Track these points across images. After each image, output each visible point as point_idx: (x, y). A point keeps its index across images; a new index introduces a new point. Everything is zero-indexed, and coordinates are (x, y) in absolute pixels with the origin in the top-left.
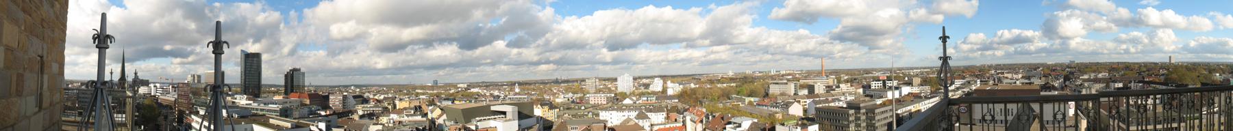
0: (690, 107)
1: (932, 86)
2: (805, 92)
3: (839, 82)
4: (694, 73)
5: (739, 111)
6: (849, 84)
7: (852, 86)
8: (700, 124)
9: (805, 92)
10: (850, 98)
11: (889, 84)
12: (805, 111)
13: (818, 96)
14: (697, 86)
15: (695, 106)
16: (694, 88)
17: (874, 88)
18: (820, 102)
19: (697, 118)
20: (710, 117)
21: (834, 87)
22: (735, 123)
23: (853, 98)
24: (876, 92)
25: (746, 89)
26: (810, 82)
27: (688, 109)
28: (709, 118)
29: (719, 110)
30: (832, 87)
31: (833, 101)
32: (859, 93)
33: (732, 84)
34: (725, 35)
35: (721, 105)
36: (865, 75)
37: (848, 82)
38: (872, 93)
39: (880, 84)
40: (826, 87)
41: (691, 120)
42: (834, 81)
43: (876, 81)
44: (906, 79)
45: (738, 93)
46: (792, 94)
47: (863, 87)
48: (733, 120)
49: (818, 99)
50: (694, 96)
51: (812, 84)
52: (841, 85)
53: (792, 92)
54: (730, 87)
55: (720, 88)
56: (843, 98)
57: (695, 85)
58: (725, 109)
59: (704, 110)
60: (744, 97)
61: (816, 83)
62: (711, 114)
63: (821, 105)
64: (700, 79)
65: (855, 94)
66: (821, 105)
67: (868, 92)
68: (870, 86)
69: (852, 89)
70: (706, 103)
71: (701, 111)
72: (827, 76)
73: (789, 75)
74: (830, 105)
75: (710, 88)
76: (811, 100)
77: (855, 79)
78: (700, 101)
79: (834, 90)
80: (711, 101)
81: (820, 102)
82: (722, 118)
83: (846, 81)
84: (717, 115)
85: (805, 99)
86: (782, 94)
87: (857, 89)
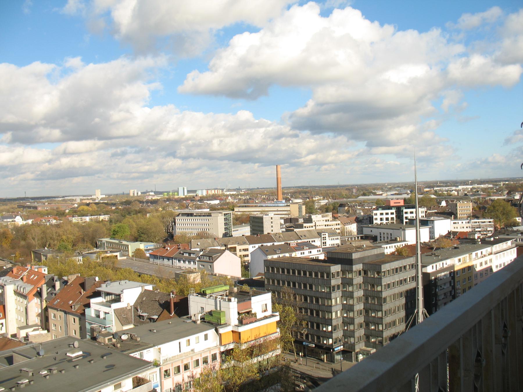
0: (14, 265)
1: (497, 218)
2: (246, 230)
3: (311, 210)
4: (23, 196)
5: (116, 269)
6: (330, 215)
7: (335, 218)
8: (36, 300)
9: (246, 230)
10: (331, 242)
11: (408, 214)
12: (246, 267)
13: (269, 238)
14: (30, 222)
15: (24, 264)
16: (23, 226)
17: (379, 222)
18: (274, 250)
19: (28, 288)
20: (58, 285)
21: (301, 221)
22: (108, 294)
23: (338, 242)
24: (382, 231)
25: (131, 227)
26: (254, 211)
27: (11, 269)
28: (54, 287)
29: (74, 268)
30: (296, 220)
31: (300, 247)
32: (350, 233)
33: (102, 217)
34: (97, 120)
35: (79, 260)
36: (361, 198)
37: (327, 211)
38: (375, 232)
39: (391, 214)
40: (286, 221)
41: (17, 293)
42: (300, 209)
43: (384, 208)
44: (444, 204)
45: (114, 234)
46: (221, 236)
47: (358, 221)
48: (103, 288)
49: (269, 244)
50: (23, 243)
51: (259, 215)
52: (313, 217)
53: (221, 231)
54: (98, 222)
55: (77, 225)
56: (318, 242)
57: (25, 218)
58: (88, 265)
59: (45, 271)
60: (124, 243)
61: (266, 213)
62: (60, 279)
63: (275, 256)
64: (36, 208)
65: (342, 234)
66: (275, 256)
67: (367, 231)
68: (370, 220)
69: (336, 225)
70: (49, 255)
71: (39, 274)
72: (287, 200)
73: (214, 197)
74: (294, 255)
75: (58, 226)
76: (257, 246)
77: (342, 205)
78: (35, 253)
79: (301, 226)
80: (59, 251)
81: (274, 250)
82: (83, 285)
83: (325, 210)
84: (71, 278)
85: (244, 243)
86: (202, 236)
87: (345, 224)
